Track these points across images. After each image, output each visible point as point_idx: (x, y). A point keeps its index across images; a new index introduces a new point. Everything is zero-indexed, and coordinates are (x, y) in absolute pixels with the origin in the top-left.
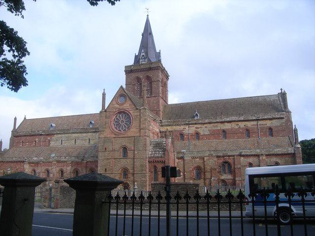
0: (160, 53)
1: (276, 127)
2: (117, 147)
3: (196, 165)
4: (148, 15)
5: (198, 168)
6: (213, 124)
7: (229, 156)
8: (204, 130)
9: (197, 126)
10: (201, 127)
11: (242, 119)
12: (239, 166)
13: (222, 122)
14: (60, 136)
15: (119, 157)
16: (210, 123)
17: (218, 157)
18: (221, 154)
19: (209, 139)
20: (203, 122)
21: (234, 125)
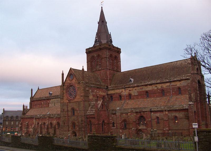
0: (110, 34)
1: (184, 86)
2: (70, 109)
3: (123, 119)
4: (102, 7)
5: (125, 121)
6: (140, 87)
7: (144, 112)
8: (134, 92)
9: (129, 89)
10: (132, 90)
11: (159, 82)
12: (150, 119)
13: (146, 85)
14: (53, 100)
15: (71, 115)
16: (138, 86)
17: (136, 112)
18: (138, 111)
19: (138, 98)
20: (133, 86)
21: (154, 87)
